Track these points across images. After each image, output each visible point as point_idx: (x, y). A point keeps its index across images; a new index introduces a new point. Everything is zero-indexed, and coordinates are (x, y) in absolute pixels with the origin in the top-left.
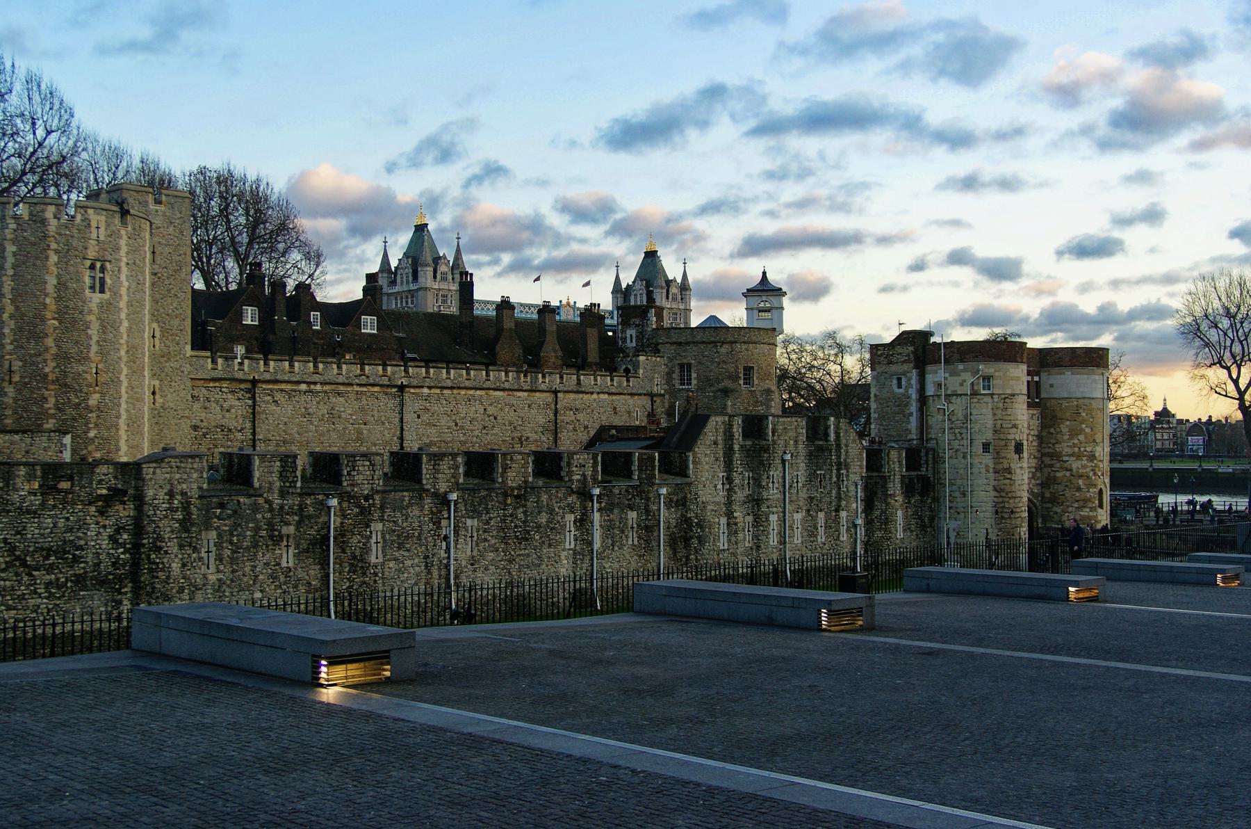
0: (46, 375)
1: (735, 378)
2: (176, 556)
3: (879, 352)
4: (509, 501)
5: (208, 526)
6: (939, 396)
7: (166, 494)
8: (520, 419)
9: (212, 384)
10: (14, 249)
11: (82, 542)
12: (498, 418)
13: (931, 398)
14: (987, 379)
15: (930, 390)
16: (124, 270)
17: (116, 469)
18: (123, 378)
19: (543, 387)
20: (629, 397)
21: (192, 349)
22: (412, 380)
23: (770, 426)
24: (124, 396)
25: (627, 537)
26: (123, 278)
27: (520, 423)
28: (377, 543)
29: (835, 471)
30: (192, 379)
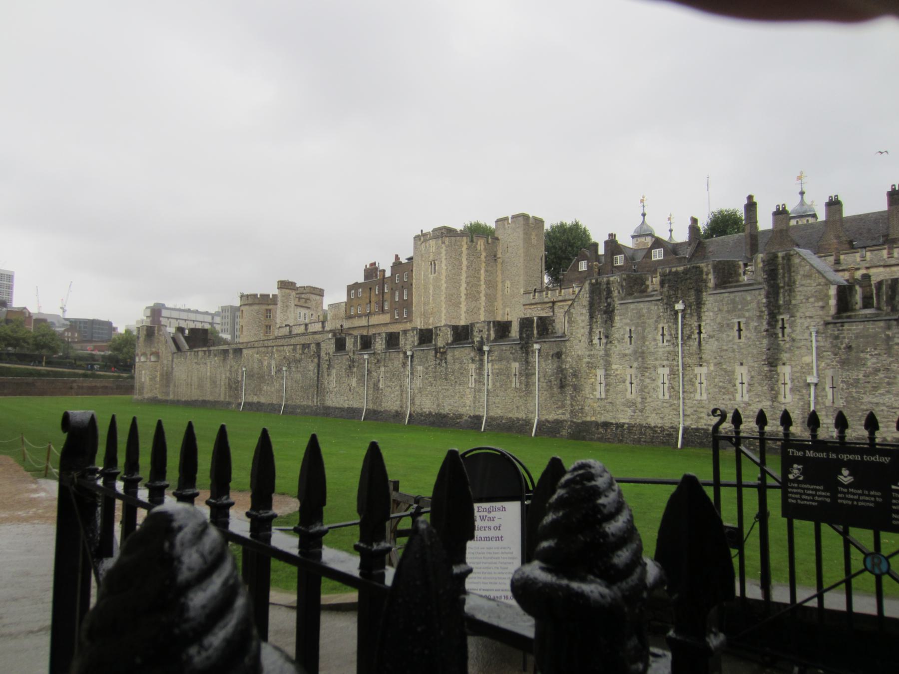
4: (438, 356)
5: (334, 368)
9: (533, 307)
18: (443, 309)
25: (511, 382)
26: (443, 265)
30: (524, 305)
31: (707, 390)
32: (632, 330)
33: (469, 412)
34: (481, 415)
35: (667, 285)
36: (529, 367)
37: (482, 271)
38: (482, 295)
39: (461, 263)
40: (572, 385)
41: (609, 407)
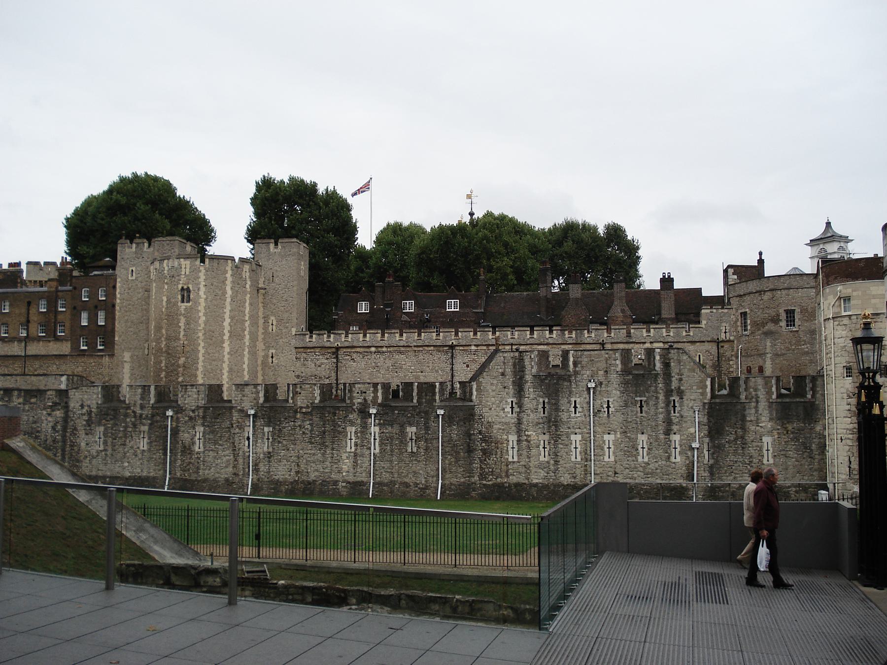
1: (776, 320)
2: (84, 439)
5: (99, 424)
7: (80, 406)
9: (309, 351)
11: (39, 429)
14: (847, 299)
16: (203, 289)
17: (56, 392)
18: (200, 348)
19: (589, 341)
23: (571, 359)
24: (201, 358)
25: (406, 445)
26: (202, 293)
29: (661, 397)
30: (296, 348)
31: (614, 453)
32: (546, 401)
33: (346, 478)
34: (365, 480)
35: (579, 365)
36: (429, 432)
37: (247, 304)
38: (246, 333)
39: (224, 293)
40: (481, 450)
41: (523, 470)
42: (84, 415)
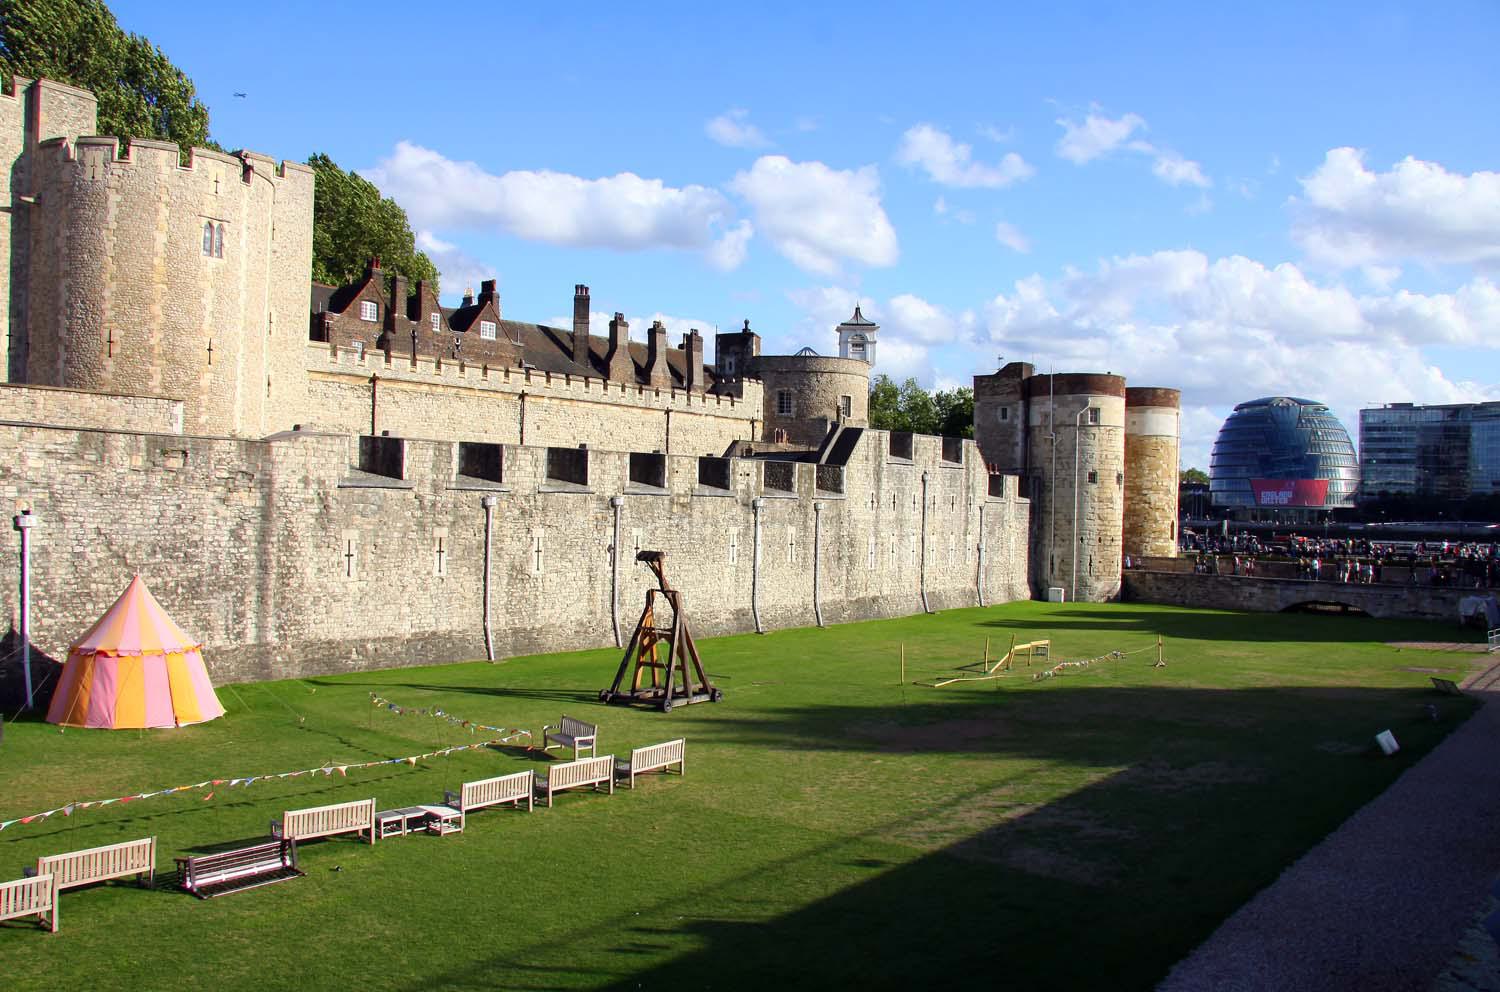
0: (152, 348)
3: (984, 384)
4: (675, 510)
6: (1046, 427)
7: (299, 481)
8: (634, 436)
9: (330, 379)
10: (119, 198)
11: (197, 538)
12: (614, 434)
13: (1037, 429)
15: (1036, 420)
16: (245, 233)
17: (240, 445)
18: (239, 356)
19: (656, 405)
20: (732, 421)
21: (312, 338)
22: (532, 389)
24: (240, 378)
27: (634, 441)
28: (538, 551)
29: (964, 491)
42: (313, 501)
